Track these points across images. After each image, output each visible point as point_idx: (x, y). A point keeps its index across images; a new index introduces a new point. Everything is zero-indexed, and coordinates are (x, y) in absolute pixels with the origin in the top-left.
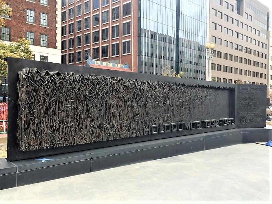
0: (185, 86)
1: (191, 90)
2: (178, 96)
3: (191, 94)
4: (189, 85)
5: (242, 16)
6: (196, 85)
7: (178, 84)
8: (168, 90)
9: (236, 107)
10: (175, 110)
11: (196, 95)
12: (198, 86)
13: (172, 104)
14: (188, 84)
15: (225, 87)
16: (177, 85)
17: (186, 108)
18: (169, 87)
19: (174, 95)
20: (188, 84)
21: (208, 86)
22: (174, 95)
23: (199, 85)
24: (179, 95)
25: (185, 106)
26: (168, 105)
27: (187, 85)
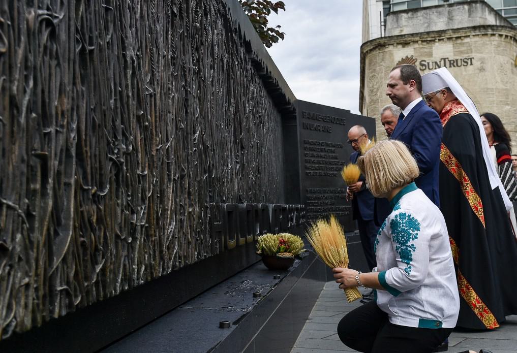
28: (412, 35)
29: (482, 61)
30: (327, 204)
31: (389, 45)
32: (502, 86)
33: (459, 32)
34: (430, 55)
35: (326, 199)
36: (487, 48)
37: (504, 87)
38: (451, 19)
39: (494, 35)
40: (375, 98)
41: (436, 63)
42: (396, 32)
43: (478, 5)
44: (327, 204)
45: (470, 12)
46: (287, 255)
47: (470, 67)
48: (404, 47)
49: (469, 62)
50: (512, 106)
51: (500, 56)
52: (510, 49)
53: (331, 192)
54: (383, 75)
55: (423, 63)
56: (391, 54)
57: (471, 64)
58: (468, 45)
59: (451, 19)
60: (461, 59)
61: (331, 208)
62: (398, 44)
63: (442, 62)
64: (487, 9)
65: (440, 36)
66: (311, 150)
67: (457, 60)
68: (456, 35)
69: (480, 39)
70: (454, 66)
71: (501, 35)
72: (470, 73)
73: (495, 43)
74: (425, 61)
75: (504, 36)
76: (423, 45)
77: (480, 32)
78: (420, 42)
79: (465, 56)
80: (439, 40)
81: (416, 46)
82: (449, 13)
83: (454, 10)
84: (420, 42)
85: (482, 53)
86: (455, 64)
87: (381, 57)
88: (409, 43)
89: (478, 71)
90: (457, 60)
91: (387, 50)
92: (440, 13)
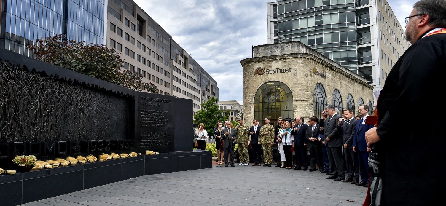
0: (47, 76)
1: (61, 86)
2: (30, 92)
3: (58, 93)
4: (55, 77)
5: (145, 38)
6: (70, 79)
7: (30, 69)
8: (5, 75)
9: (136, 124)
10: (21, 117)
11: (70, 96)
12: (73, 81)
13: (16, 106)
14: (54, 75)
15: (120, 92)
16: (29, 71)
17: (48, 116)
18: (9, 71)
19: (21, 88)
20: (54, 75)
21: (93, 85)
22: (21, 88)
23: (75, 80)
24: (33, 91)
25: (46, 112)
26: (4, 105)
27: (52, 76)
28: (263, 57)
29: (295, 70)
30: (154, 139)
31: (252, 62)
32: (304, 82)
33: (285, 56)
34: (271, 67)
35: (154, 137)
36: (298, 64)
37: (306, 83)
38: (283, 50)
39: (301, 58)
40: (245, 87)
41: (273, 70)
42: (257, 56)
43: (296, 43)
44: (154, 139)
45: (292, 46)
46: (23, 165)
47: (289, 73)
48: (259, 63)
49: (289, 70)
50: (310, 92)
51: (305, 68)
52: (310, 65)
53: (157, 134)
54: (249, 76)
55: (267, 70)
56: (253, 66)
57: (290, 72)
58: (289, 62)
59: (283, 50)
60: (285, 69)
61: (157, 141)
62: (256, 61)
63: (277, 70)
64: (300, 45)
65: (276, 58)
66: (144, 114)
67: (283, 70)
68: (283, 58)
69: (295, 60)
70: (282, 72)
71: (305, 58)
72: (290, 75)
73: (302, 61)
74: (268, 70)
75: (307, 59)
76: (267, 62)
77: (294, 56)
78: (266, 61)
79: (287, 67)
80: (275, 60)
81: (265, 62)
82: (282, 47)
83: (284, 46)
84: (266, 61)
85: (295, 66)
86: (282, 71)
87: (248, 67)
88: (261, 61)
89: (293, 75)
90: (283, 70)
91: (251, 64)
92: (278, 47)
